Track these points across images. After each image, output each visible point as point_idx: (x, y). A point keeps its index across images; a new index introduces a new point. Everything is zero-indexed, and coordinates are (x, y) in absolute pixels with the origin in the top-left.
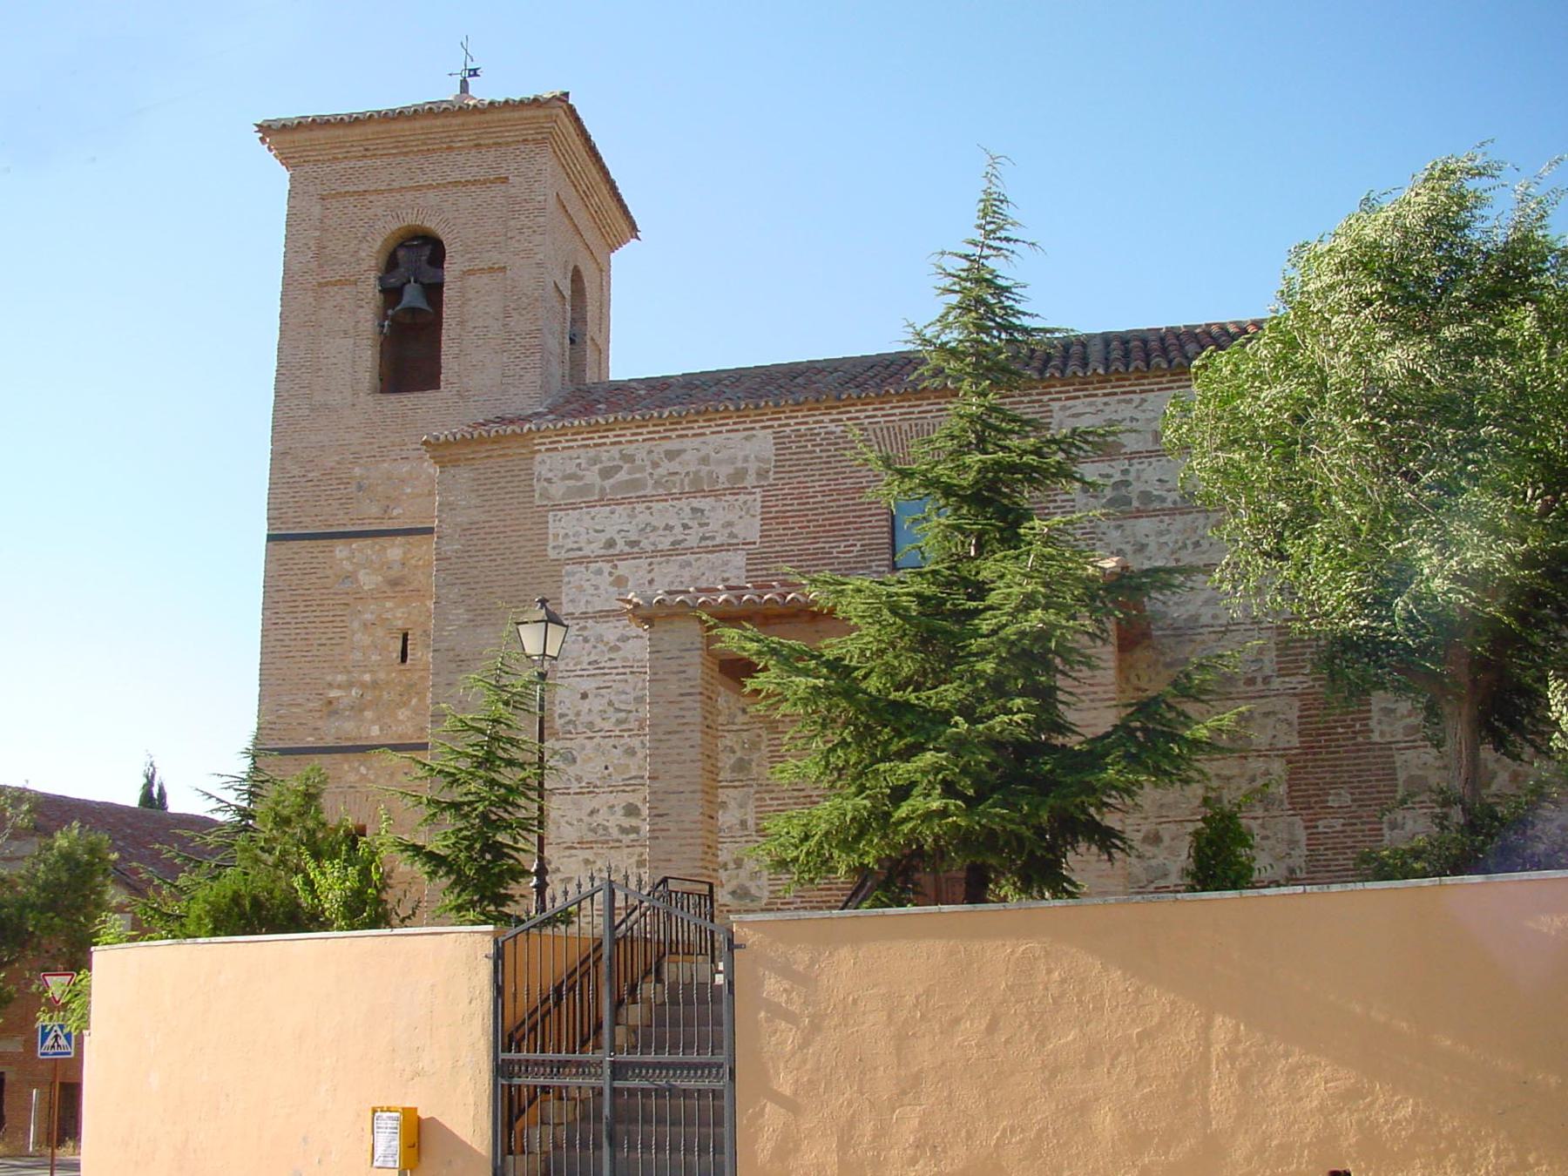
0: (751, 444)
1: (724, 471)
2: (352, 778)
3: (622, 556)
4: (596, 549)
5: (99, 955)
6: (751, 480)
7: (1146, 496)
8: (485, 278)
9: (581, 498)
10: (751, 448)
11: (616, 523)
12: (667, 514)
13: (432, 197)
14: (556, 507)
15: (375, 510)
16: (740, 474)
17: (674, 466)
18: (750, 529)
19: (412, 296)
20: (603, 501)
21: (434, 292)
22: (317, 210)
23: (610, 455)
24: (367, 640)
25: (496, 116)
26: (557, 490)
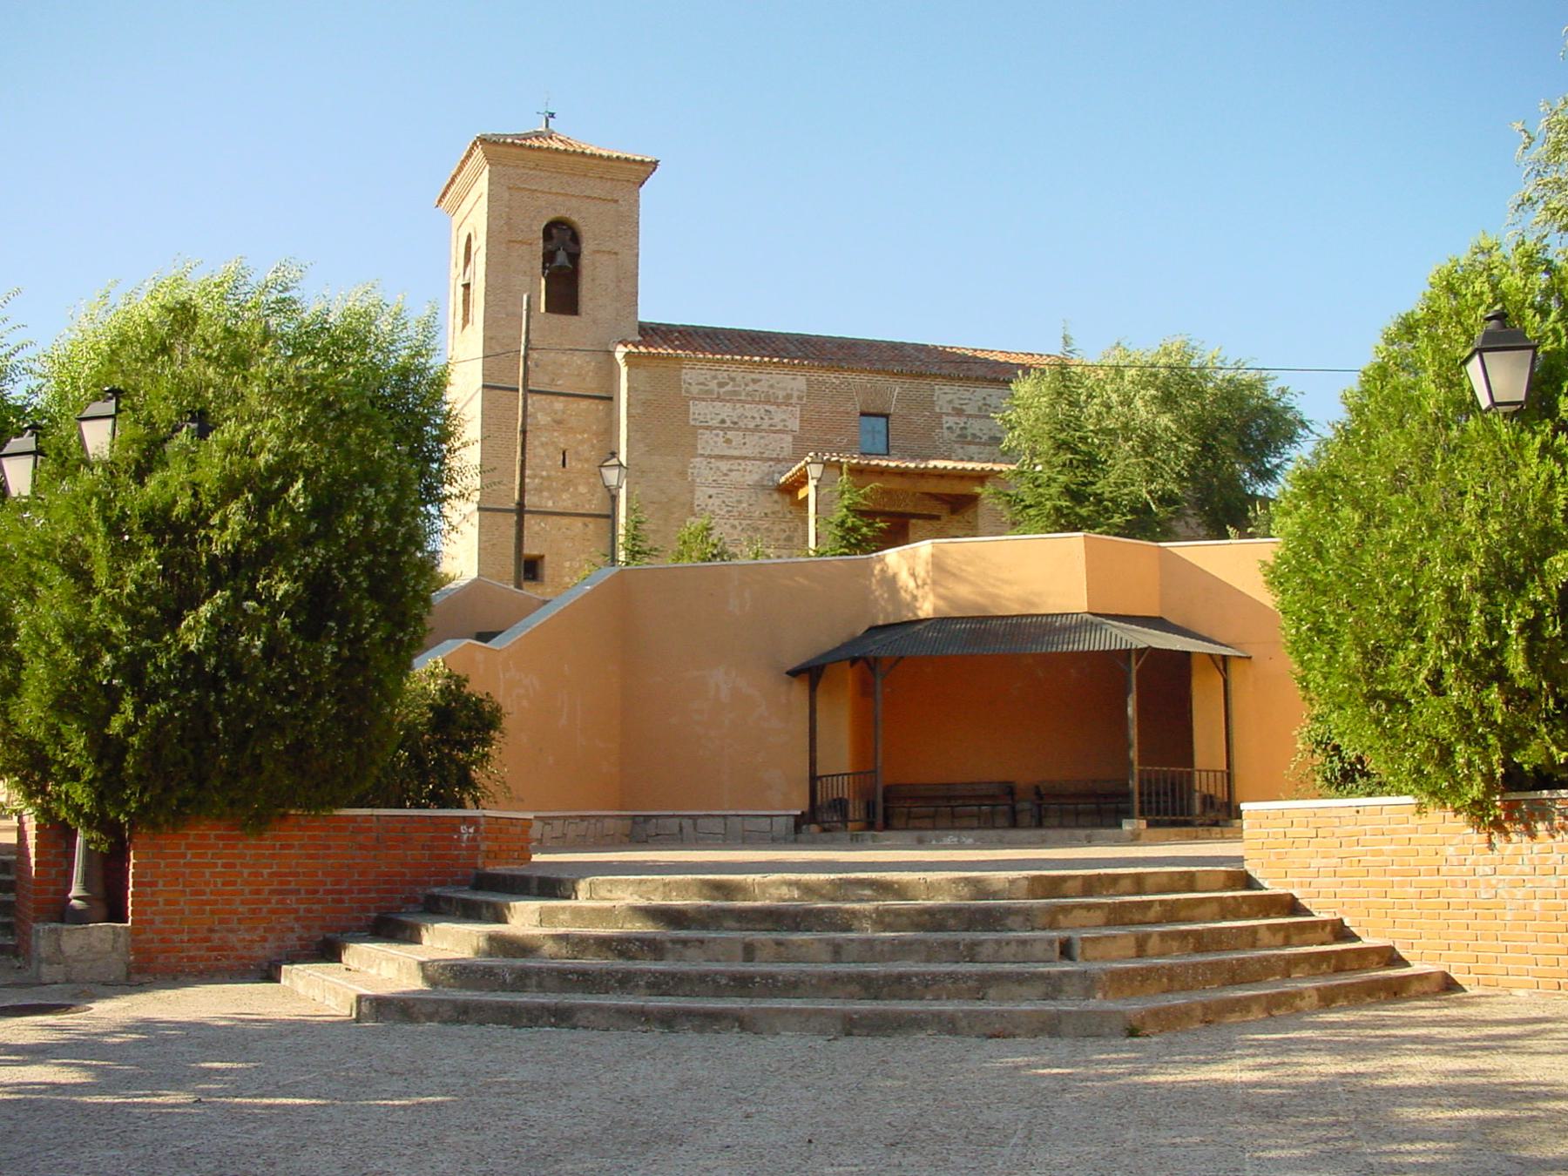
0: (794, 382)
1: (781, 394)
2: (537, 528)
3: (729, 428)
4: (715, 423)
5: (1076, 541)
6: (794, 401)
7: (974, 435)
8: (606, 257)
9: (706, 396)
10: (794, 384)
11: (726, 411)
12: (751, 410)
13: (574, 203)
14: (694, 399)
15: (546, 380)
16: (789, 396)
17: (756, 387)
18: (795, 425)
19: (561, 258)
20: (719, 398)
21: (575, 257)
22: (506, 195)
23: (722, 377)
24: (543, 453)
25: (617, 164)
26: (695, 389)
